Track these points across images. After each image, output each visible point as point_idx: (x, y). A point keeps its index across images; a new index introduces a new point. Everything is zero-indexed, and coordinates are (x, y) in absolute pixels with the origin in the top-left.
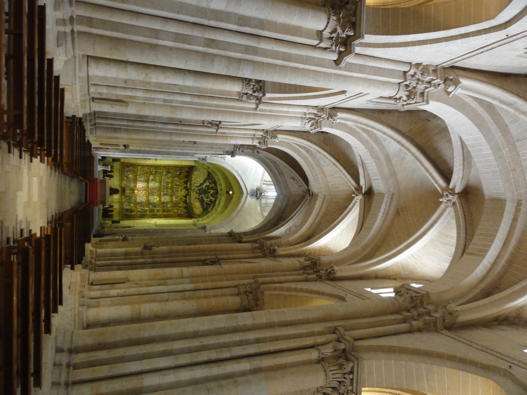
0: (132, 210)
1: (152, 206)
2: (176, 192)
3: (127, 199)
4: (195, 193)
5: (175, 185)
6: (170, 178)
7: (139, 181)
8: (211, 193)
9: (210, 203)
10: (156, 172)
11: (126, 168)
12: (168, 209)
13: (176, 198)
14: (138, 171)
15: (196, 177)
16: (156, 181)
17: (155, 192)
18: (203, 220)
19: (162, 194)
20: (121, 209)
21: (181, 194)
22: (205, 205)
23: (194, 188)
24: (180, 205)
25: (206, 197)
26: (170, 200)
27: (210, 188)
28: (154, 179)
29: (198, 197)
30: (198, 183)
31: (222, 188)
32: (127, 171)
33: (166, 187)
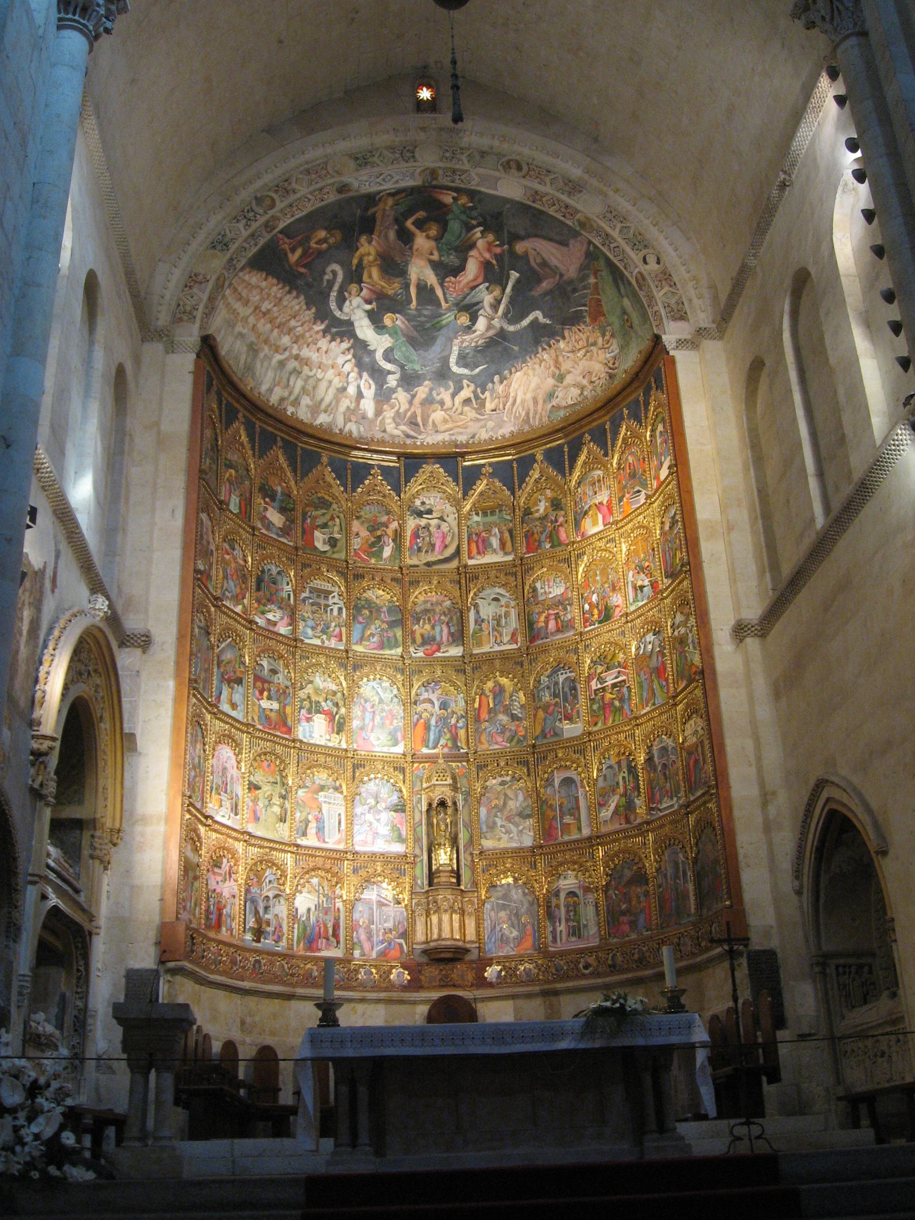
0: (614, 875)
1: (569, 718)
2: (432, 546)
3: (515, 933)
4: (437, 415)
5: (378, 554)
6: (318, 584)
7: (350, 834)
8: (431, 278)
9: (514, 275)
10: (262, 684)
11: (224, 933)
12: (587, 584)
13: (484, 546)
14: (251, 828)
15: (303, 388)
16: (349, 698)
17: (444, 706)
18: (666, 277)
19: (456, 651)
20: (614, 968)
21: (449, 509)
22: (525, 322)
23: (398, 417)
24: (542, 507)
25: (464, 320)
26: (498, 590)
27: (393, 288)
28: (331, 716)
29: (466, 393)
30: (352, 390)
31: (392, 149)
32: (259, 933)
33: (392, 625)
